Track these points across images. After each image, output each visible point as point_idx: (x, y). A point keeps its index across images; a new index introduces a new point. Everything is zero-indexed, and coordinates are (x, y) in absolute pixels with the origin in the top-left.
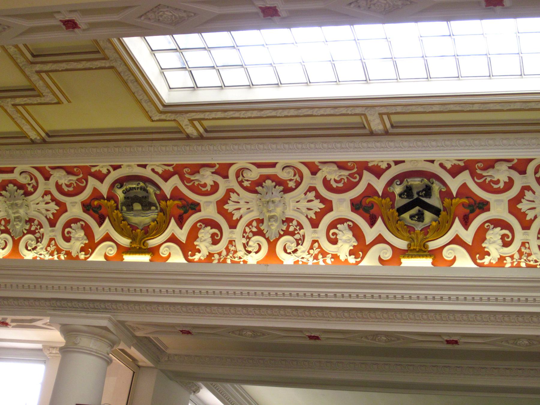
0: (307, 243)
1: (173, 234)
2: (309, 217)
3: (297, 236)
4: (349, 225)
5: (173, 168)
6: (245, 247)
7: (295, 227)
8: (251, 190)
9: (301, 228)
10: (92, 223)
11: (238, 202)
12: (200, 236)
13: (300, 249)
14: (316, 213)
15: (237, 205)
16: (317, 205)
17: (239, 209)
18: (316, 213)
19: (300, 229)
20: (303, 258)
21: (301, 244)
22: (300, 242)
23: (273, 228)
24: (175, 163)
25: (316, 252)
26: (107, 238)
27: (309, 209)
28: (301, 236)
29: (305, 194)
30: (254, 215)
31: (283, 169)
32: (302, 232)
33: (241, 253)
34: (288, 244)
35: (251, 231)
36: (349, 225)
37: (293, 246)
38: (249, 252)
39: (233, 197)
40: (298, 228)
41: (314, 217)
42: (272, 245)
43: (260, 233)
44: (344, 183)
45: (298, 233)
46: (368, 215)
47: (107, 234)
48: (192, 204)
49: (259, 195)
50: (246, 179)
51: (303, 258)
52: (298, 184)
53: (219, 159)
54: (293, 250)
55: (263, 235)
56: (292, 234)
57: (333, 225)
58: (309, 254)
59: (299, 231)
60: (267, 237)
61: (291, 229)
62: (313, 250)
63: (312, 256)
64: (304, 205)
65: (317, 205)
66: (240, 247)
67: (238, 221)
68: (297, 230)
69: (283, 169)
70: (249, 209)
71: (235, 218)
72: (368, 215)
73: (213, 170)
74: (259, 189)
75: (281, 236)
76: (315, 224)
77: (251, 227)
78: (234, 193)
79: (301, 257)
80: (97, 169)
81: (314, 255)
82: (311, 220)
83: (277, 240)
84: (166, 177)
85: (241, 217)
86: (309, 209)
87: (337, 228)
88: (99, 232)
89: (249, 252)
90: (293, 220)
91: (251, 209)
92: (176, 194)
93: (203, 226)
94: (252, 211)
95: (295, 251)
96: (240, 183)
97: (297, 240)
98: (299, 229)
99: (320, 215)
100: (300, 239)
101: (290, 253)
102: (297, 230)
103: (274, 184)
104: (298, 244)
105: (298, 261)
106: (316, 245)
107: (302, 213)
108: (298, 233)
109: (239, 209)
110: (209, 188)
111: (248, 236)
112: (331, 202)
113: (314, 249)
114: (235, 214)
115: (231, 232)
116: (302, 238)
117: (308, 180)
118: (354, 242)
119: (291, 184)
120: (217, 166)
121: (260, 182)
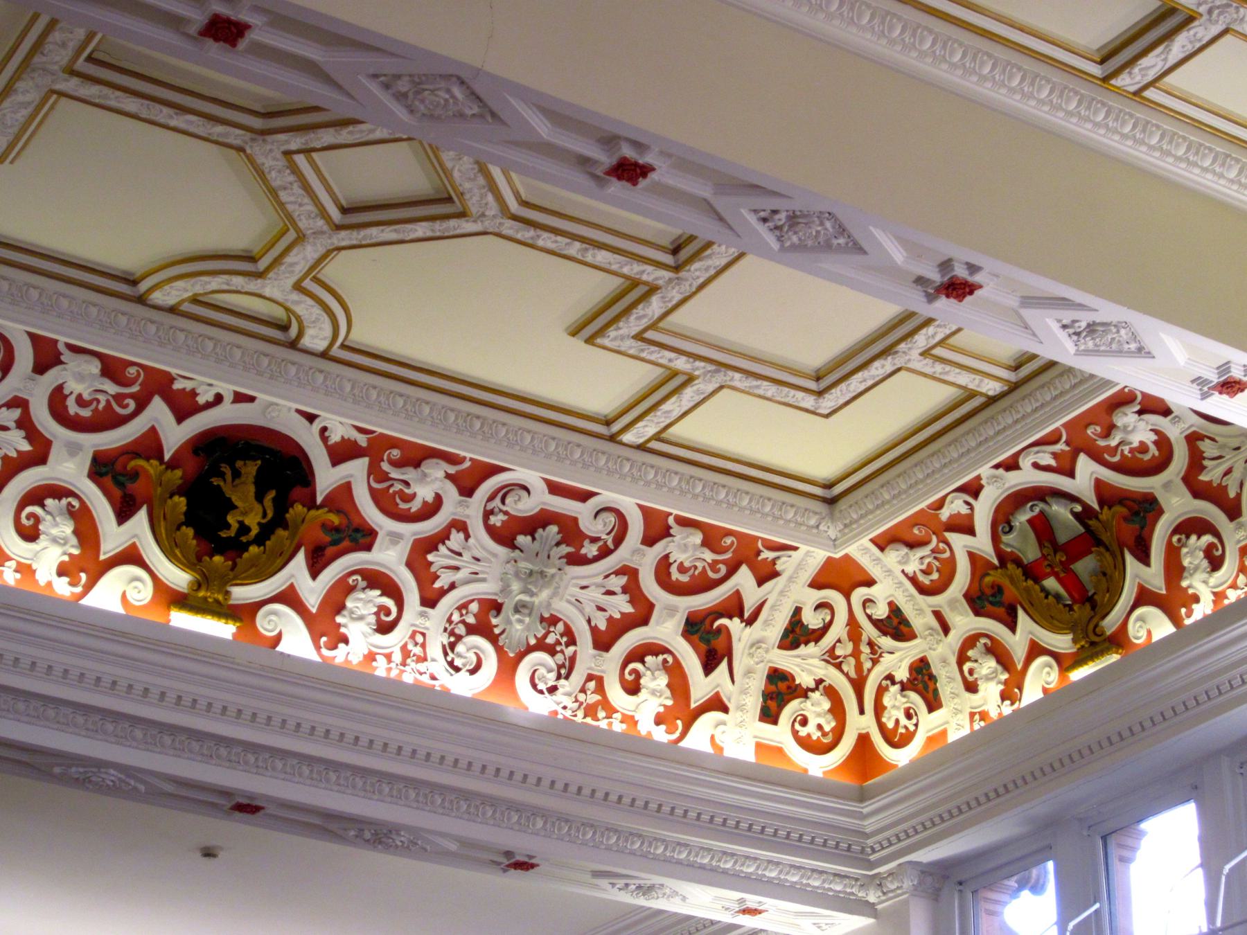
0: (578, 677)
1: (292, 586)
2: (593, 624)
3: (559, 657)
4: (665, 661)
5: (369, 440)
6: (446, 654)
7: (558, 637)
8: (505, 536)
9: (572, 641)
10: (102, 509)
11: (460, 554)
12: (349, 604)
13: (563, 686)
14: (610, 620)
15: (453, 559)
16: (621, 605)
17: (457, 568)
18: (610, 620)
19: (567, 645)
20: (565, 708)
21: (563, 676)
22: (563, 671)
23: (518, 629)
24: (379, 430)
25: (593, 698)
26: (131, 556)
27: (601, 609)
28: (565, 659)
29: (607, 577)
30: (487, 589)
31: (596, 516)
32: (572, 649)
33: (438, 665)
34: (542, 671)
35: (463, 622)
36: (665, 661)
37: (551, 678)
38: (457, 669)
39: (456, 539)
40: (565, 639)
41: (603, 626)
42: (508, 666)
43: (482, 628)
44: (693, 576)
45: (562, 652)
46: (703, 647)
47: (134, 546)
48: (357, 530)
49: (517, 552)
50: (505, 508)
51: (565, 708)
52: (605, 553)
53: (472, 452)
54: (549, 685)
55: (493, 639)
56: (551, 650)
57: (638, 654)
58: (576, 701)
59: (563, 647)
60: (501, 644)
61: (550, 640)
62: (586, 694)
63: (582, 707)
64: (596, 595)
65: (621, 605)
66: (435, 650)
67: (443, 592)
68: (561, 644)
69: (596, 516)
70: (476, 573)
71: (437, 585)
72: (703, 647)
73: (452, 470)
74: (522, 540)
75: (530, 649)
76: (603, 642)
77: (464, 612)
78: (458, 531)
79: (562, 705)
80: (188, 385)
81: (584, 705)
82: (594, 630)
83: (521, 656)
84: (341, 453)
85: (453, 586)
86: (601, 609)
87: (643, 662)
88: (113, 537)
89: (457, 669)
90: (560, 620)
91: (480, 576)
92: (342, 496)
93: (364, 584)
94: (484, 580)
95: (552, 690)
96: (487, 514)
97: (560, 667)
98: (565, 642)
99: (620, 627)
100: (563, 666)
101: (541, 692)
102: (561, 644)
103: (559, 537)
104: (559, 677)
105: (556, 713)
106: (592, 685)
107: (582, 611)
108: (562, 652)
109: (457, 568)
110: (415, 506)
111: (453, 630)
112: (651, 606)
113: (589, 693)
114: (443, 576)
115: (423, 615)
116: (567, 664)
117: (631, 551)
118: (667, 698)
119: (591, 550)
120: (467, 464)
121: (534, 524)
